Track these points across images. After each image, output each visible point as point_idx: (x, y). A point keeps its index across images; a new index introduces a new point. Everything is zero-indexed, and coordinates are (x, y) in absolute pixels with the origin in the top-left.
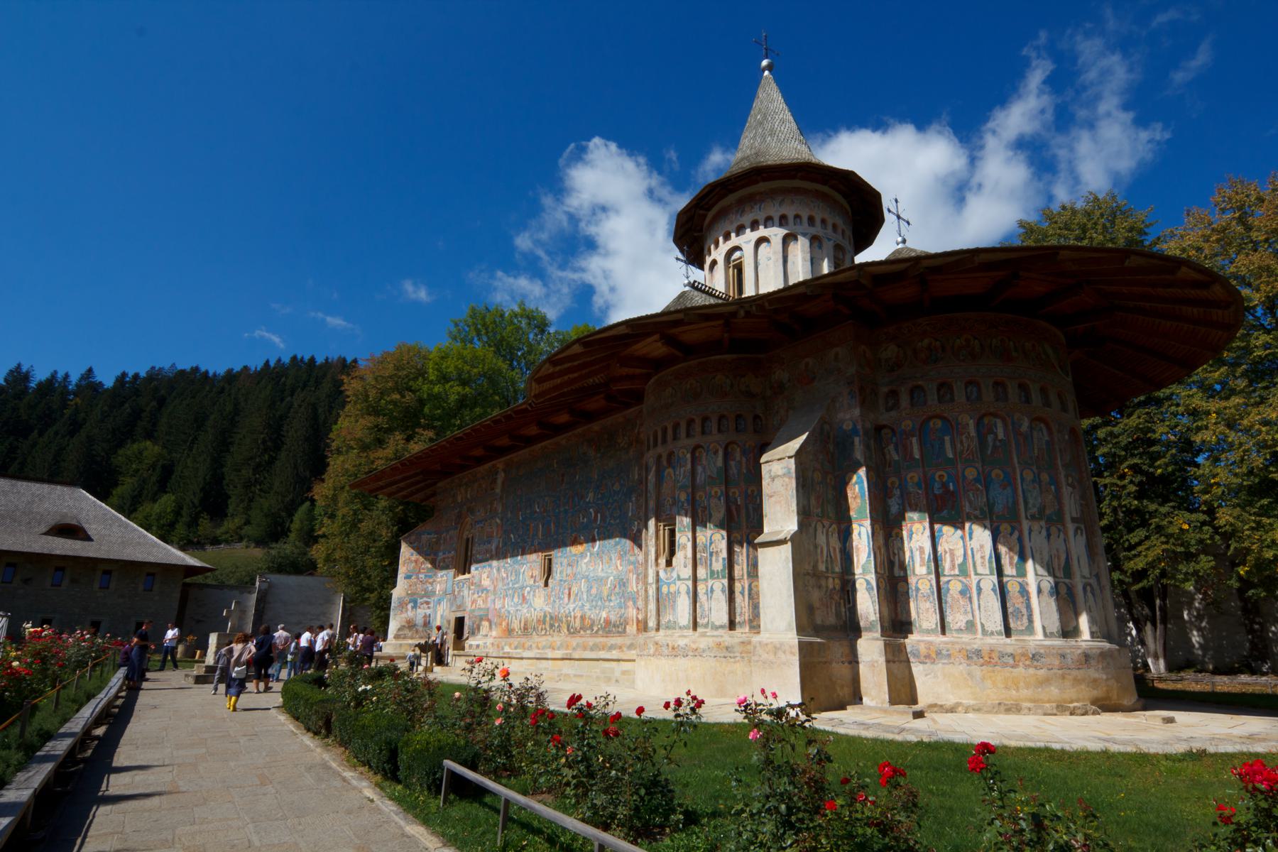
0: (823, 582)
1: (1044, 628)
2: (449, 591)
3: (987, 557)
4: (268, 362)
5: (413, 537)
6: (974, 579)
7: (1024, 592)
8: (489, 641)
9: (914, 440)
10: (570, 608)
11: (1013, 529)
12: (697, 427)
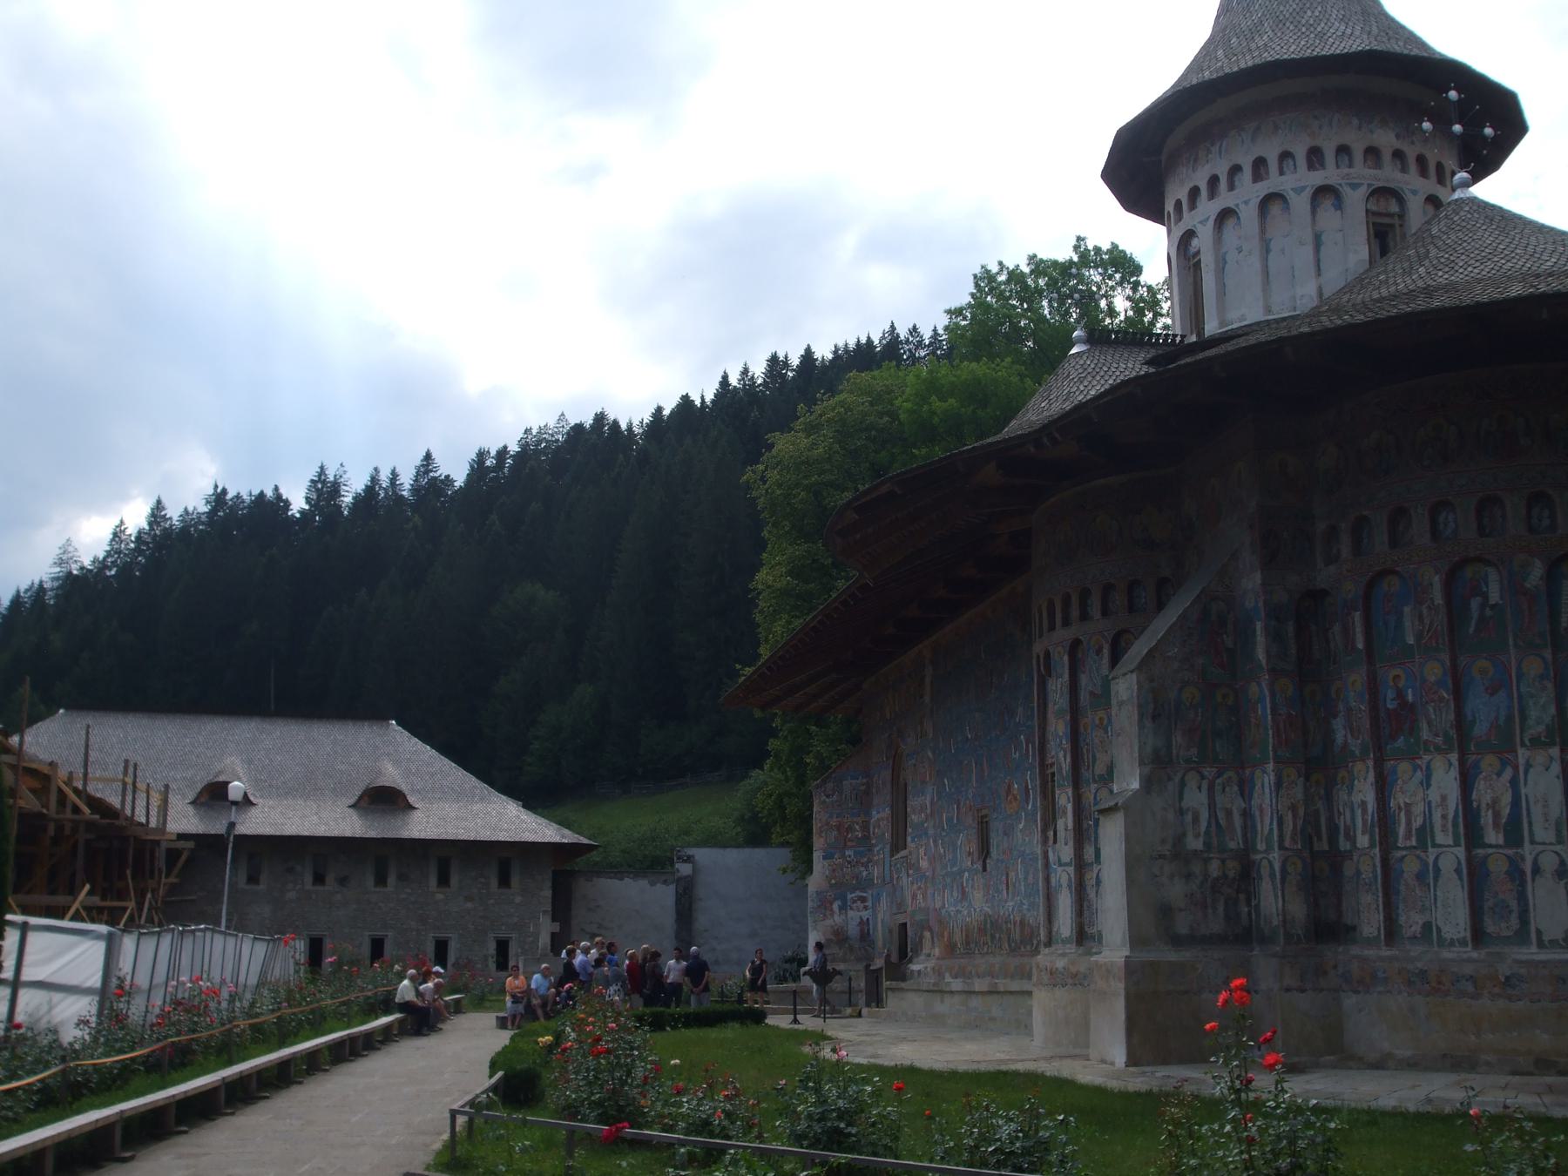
0: (1197, 868)
1: (1539, 932)
2: (888, 879)
3: (1451, 816)
4: (725, 377)
5: (830, 785)
6: (1432, 853)
7: (1516, 873)
8: (931, 964)
9: (1357, 616)
10: (1008, 906)
11: (1504, 764)
12: (1075, 613)
